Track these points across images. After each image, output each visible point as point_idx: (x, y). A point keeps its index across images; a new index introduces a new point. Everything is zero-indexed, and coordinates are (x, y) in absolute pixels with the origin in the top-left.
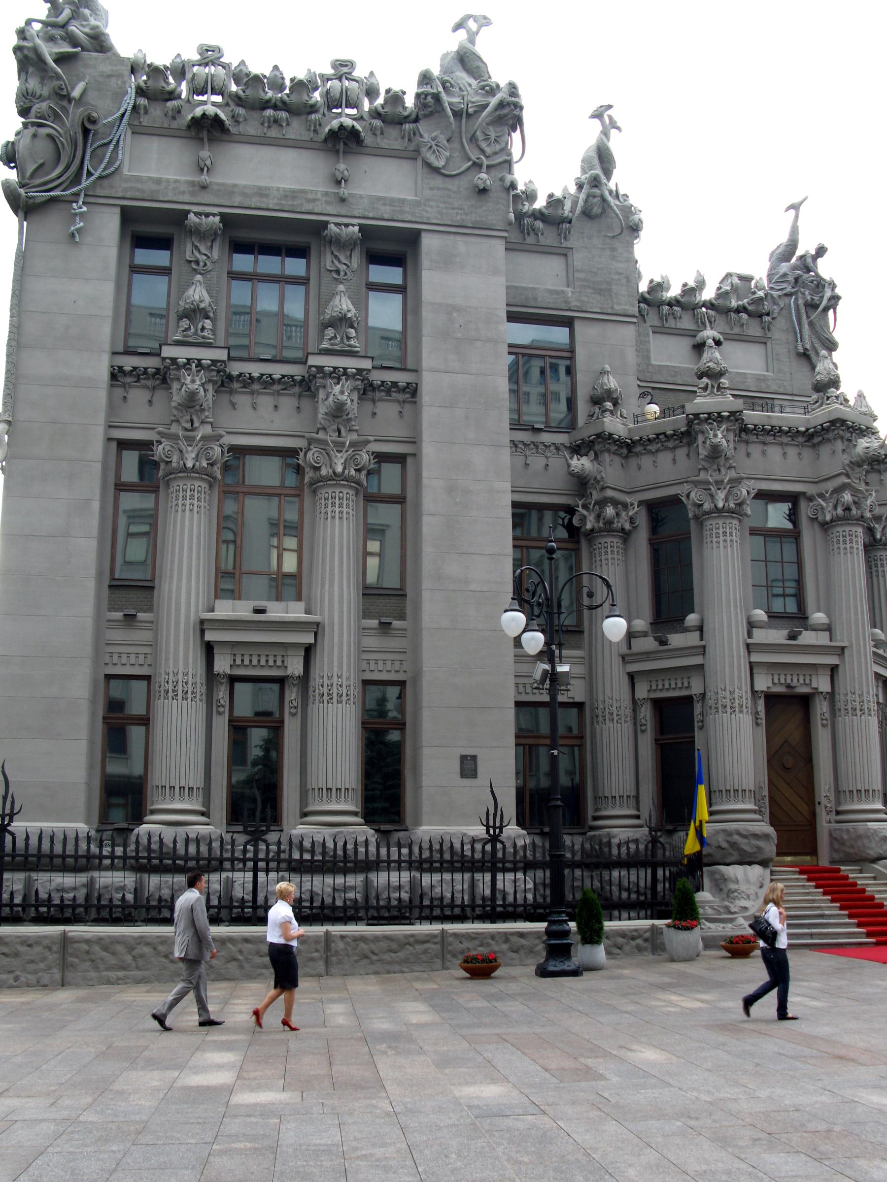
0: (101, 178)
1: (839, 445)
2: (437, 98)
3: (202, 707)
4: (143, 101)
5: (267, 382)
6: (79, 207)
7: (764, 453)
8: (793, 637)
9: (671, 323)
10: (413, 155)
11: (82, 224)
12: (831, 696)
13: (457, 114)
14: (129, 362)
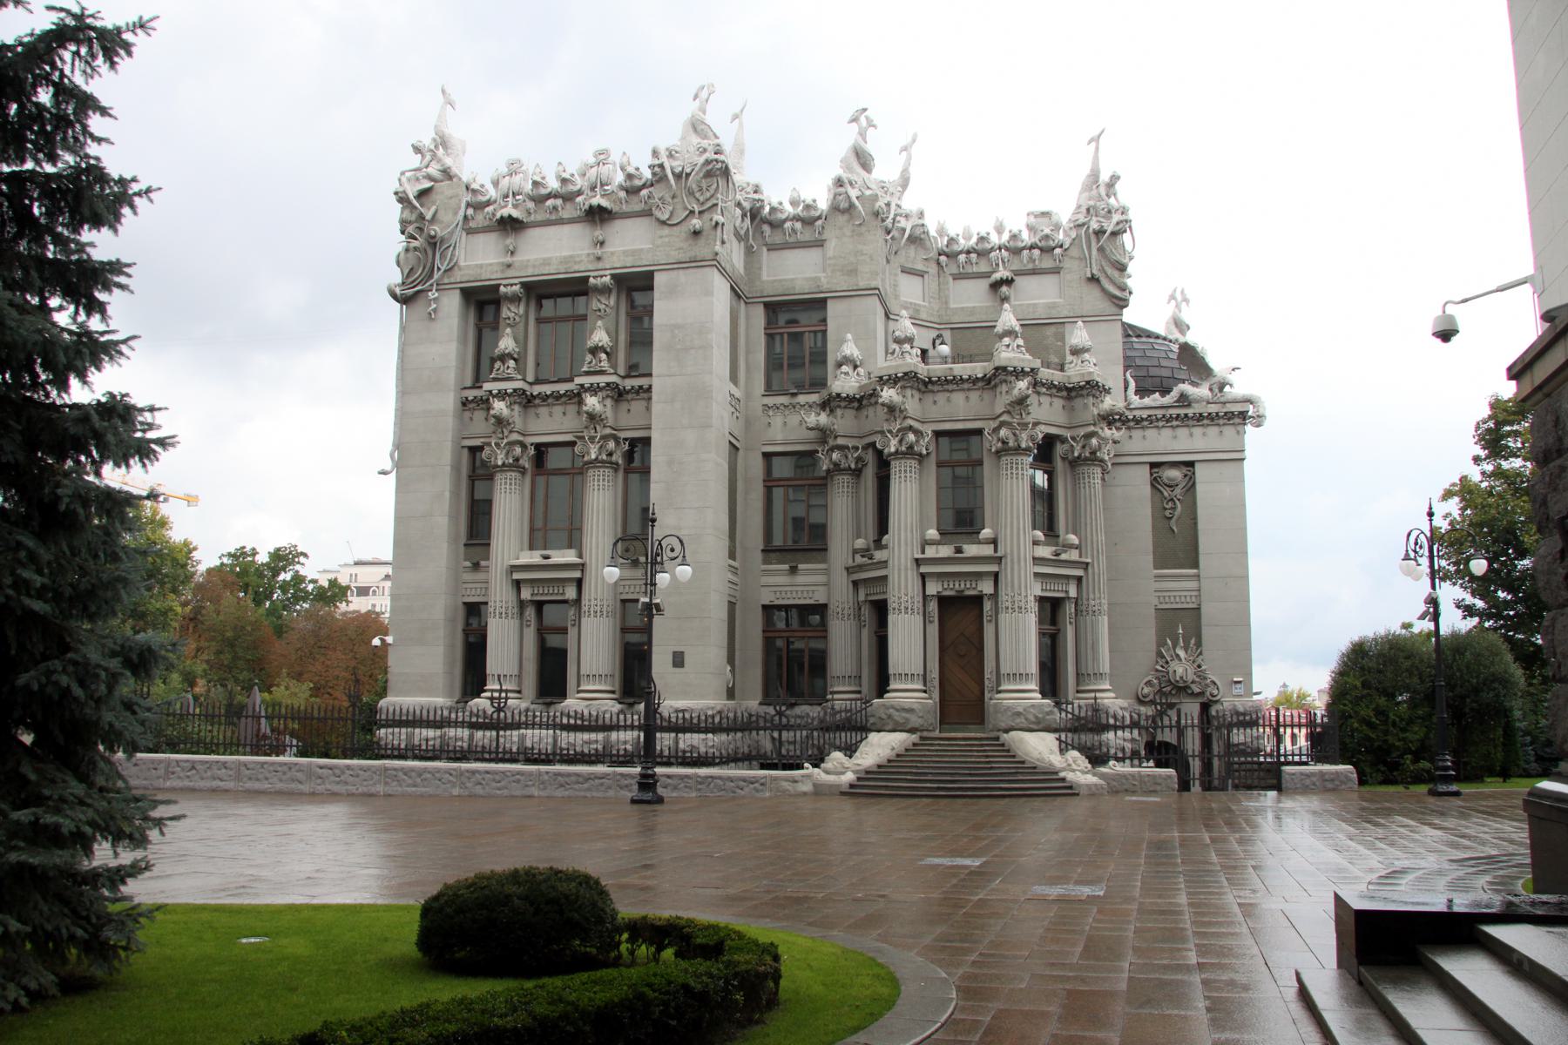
1: (1004, 388)
2: (661, 166)
3: (517, 622)
4: (470, 211)
5: (557, 397)
6: (432, 295)
7: (948, 400)
8: (959, 550)
9: (969, 269)
10: (647, 213)
12: (995, 596)
13: (678, 176)
14: (471, 394)
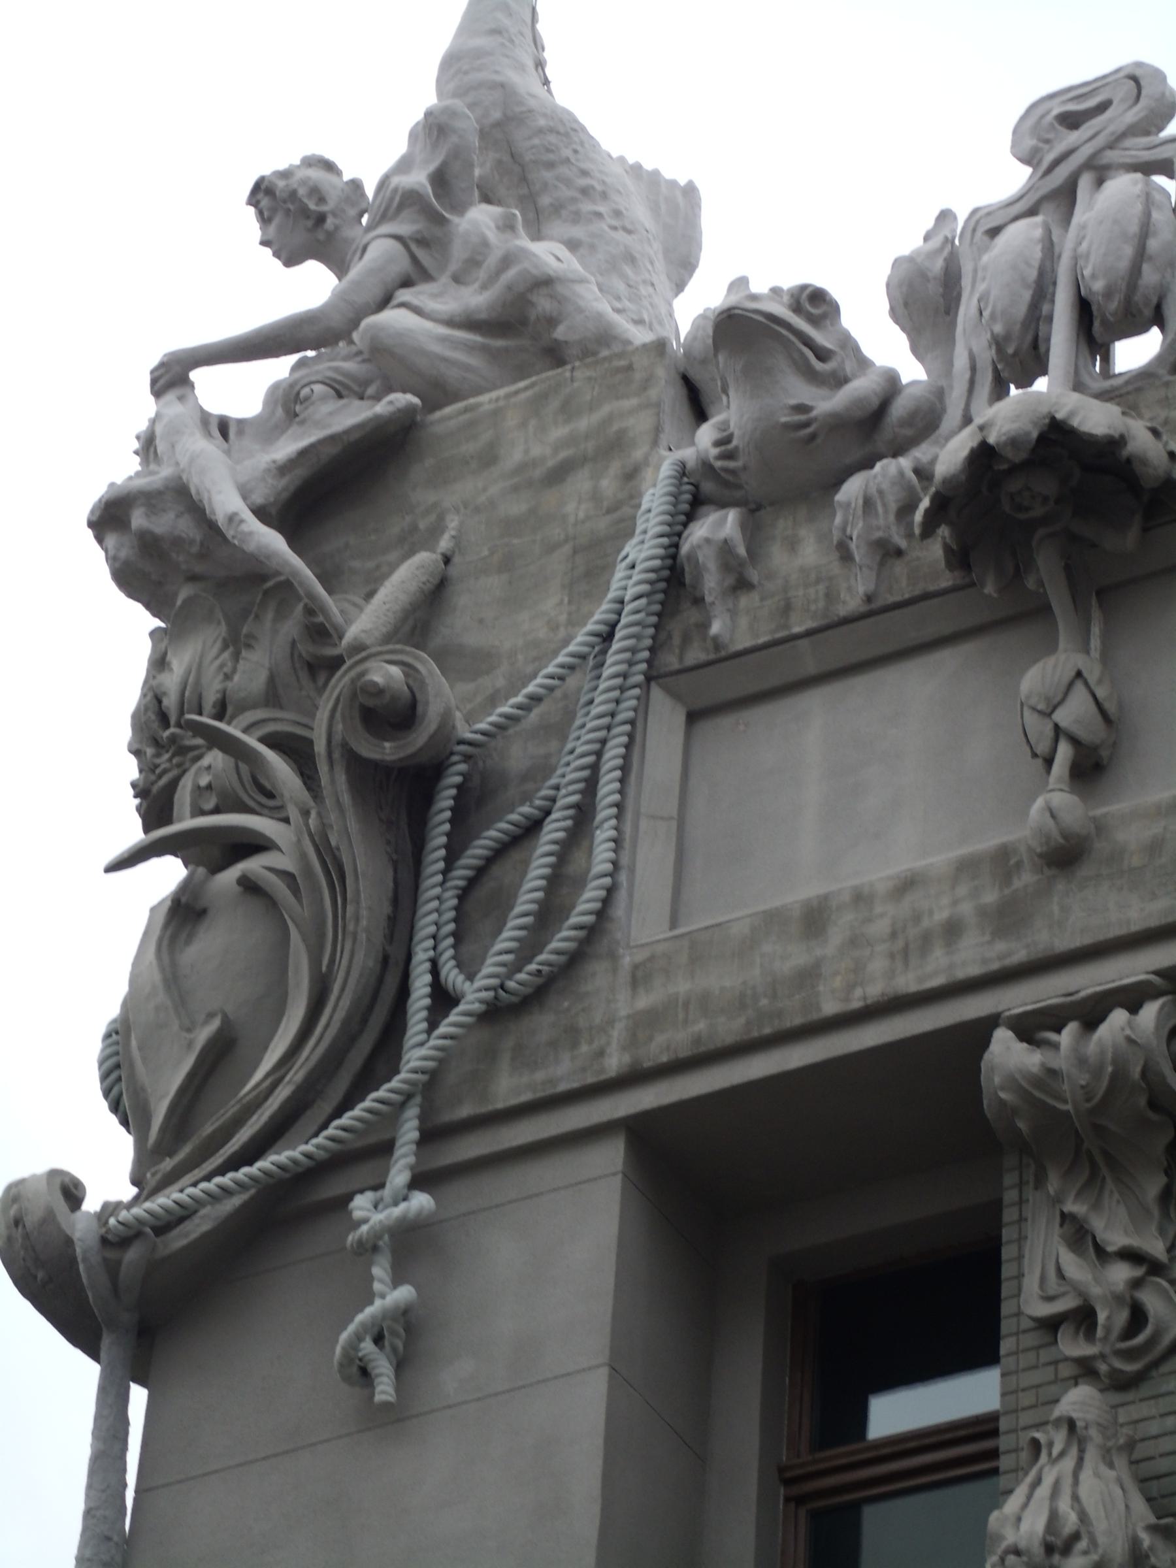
0: (498, 1012)
11: (404, 1293)
